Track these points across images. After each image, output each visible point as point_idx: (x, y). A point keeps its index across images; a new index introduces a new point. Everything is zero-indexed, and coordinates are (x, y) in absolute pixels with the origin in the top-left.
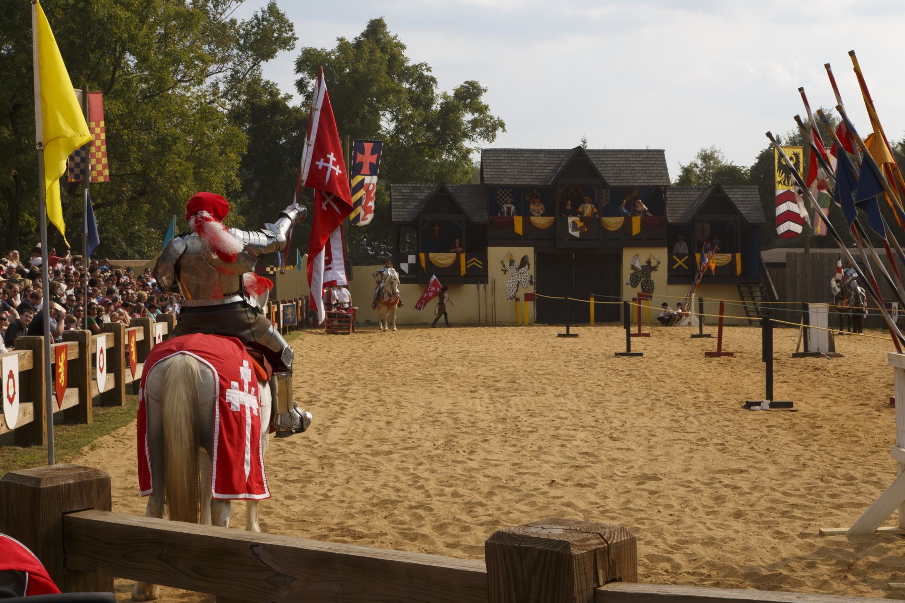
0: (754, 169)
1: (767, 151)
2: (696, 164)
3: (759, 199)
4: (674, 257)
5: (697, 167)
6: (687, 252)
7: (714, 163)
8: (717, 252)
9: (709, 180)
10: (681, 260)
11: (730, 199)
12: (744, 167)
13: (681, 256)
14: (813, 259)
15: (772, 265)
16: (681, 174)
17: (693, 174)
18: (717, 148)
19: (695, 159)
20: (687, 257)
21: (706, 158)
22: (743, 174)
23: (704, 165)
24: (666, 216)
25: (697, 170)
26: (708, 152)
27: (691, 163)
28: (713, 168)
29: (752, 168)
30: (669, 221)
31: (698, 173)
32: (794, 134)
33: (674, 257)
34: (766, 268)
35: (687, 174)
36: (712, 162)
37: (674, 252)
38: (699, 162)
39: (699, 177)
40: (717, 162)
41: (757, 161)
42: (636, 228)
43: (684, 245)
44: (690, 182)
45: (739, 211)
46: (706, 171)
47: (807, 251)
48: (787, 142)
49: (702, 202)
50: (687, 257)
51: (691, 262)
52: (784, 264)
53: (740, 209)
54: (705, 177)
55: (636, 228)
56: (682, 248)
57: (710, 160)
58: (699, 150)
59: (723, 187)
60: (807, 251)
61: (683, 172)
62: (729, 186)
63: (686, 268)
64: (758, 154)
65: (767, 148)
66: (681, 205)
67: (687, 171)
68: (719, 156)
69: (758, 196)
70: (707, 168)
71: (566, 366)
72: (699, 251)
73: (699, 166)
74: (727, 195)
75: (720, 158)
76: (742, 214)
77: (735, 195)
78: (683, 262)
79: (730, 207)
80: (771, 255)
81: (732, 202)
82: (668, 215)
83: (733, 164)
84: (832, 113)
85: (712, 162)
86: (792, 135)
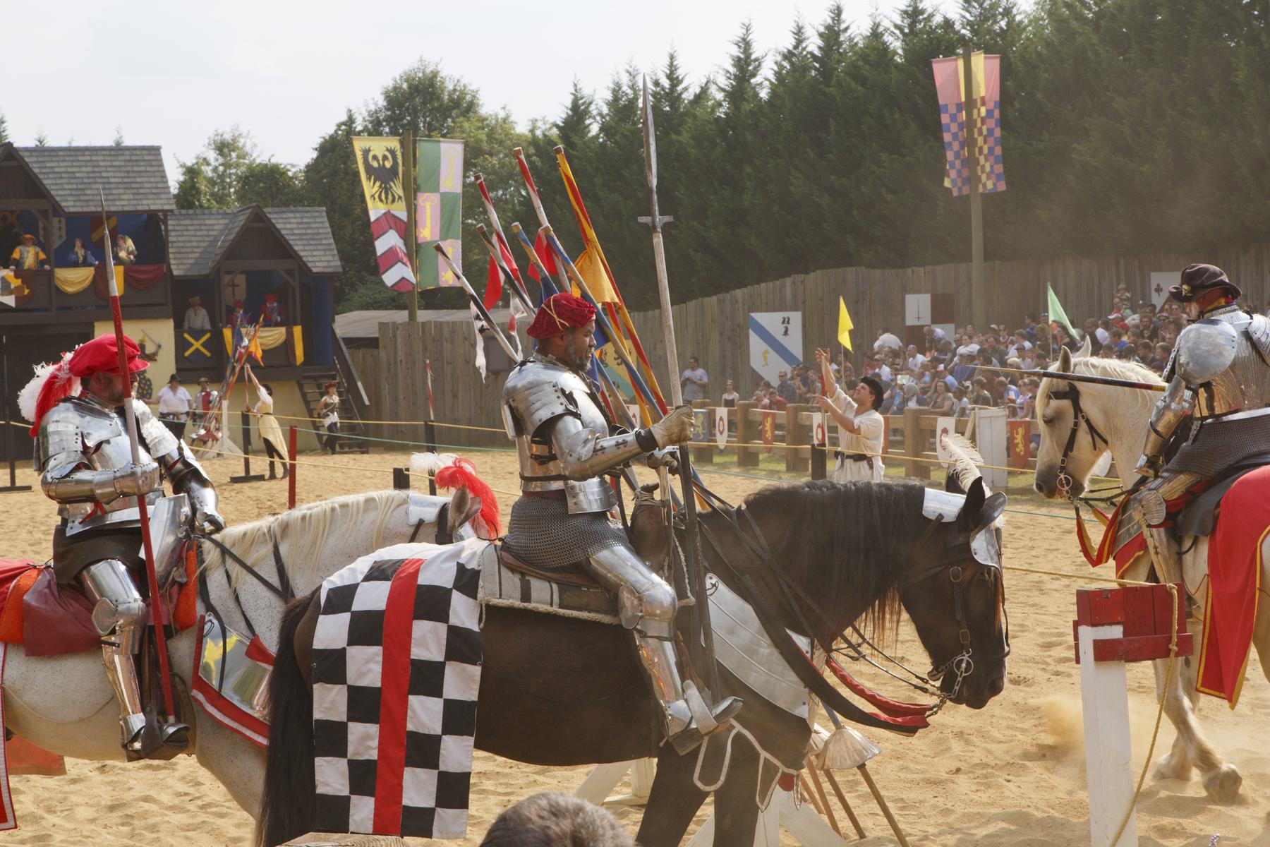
0: (311, 169)
1: (331, 137)
2: (205, 159)
3: (329, 230)
4: (186, 336)
5: (208, 164)
6: (208, 326)
7: (239, 157)
8: (262, 327)
9: (230, 187)
10: (197, 340)
11: (278, 231)
12: (293, 166)
13: (197, 334)
14: (424, 332)
15: (354, 343)
16: (182, 178)
17: (201, 179)
18: (243, 130)
19: (204, 149)
20: (208, 336)
21: (223, 147)
22: (292, 178)
23: (221, 160)
24: (169, 264)
25: (208, 171)
26: (228, 137)
27: (198, 158)
28: (237, 166)
29: (307, 166)
30: (175, 273)
31: (210, 174)
32: (376, 104)
33: (186, 336)
34: (344, 348)
35: (192, 179)
36: (234, 155)
37: (186, 327)
38: (212, 155)
39: (212, 182)
40: (242, 156)
41: (315, 155)
42: (116, 287)
43: (203, 313)
44: (198, 191)
45: (295, 252)
46: (225, 171)
47: (412, 317)
48: (364, 120)
49: (231, 237)
50: (208, 336)
51: (216, 343)
52: (376, 339)
53: (296, 248)
54: (223, 181)
55: (116, 287)
56: (200, 318)
57: (230, 151)
58: (211, 134)
59: (266, 210)
60: (412, 317)
61: (184, 174)
62: (277, 210)
63: (208, 354)
64: (317, 142)
65: (330, 130)
66: (195, 244)
67: (192, 173)
68: (246, 144)
69: (327, 225)
70: (227, 165)
71: (37, 553)
72: (231, 322)
73: (213, 163)
74: (273, 224)
75: (248, 148)
76: (300, 258)
77: (288, 223)
78: (203, 345)
79: (282, 249)
80: (349, 324)
81: (282, 235)
82: (172, 262)
83: (274, 161)
84: (439, 69)
85: (234, 155)
86: (373, 108)
